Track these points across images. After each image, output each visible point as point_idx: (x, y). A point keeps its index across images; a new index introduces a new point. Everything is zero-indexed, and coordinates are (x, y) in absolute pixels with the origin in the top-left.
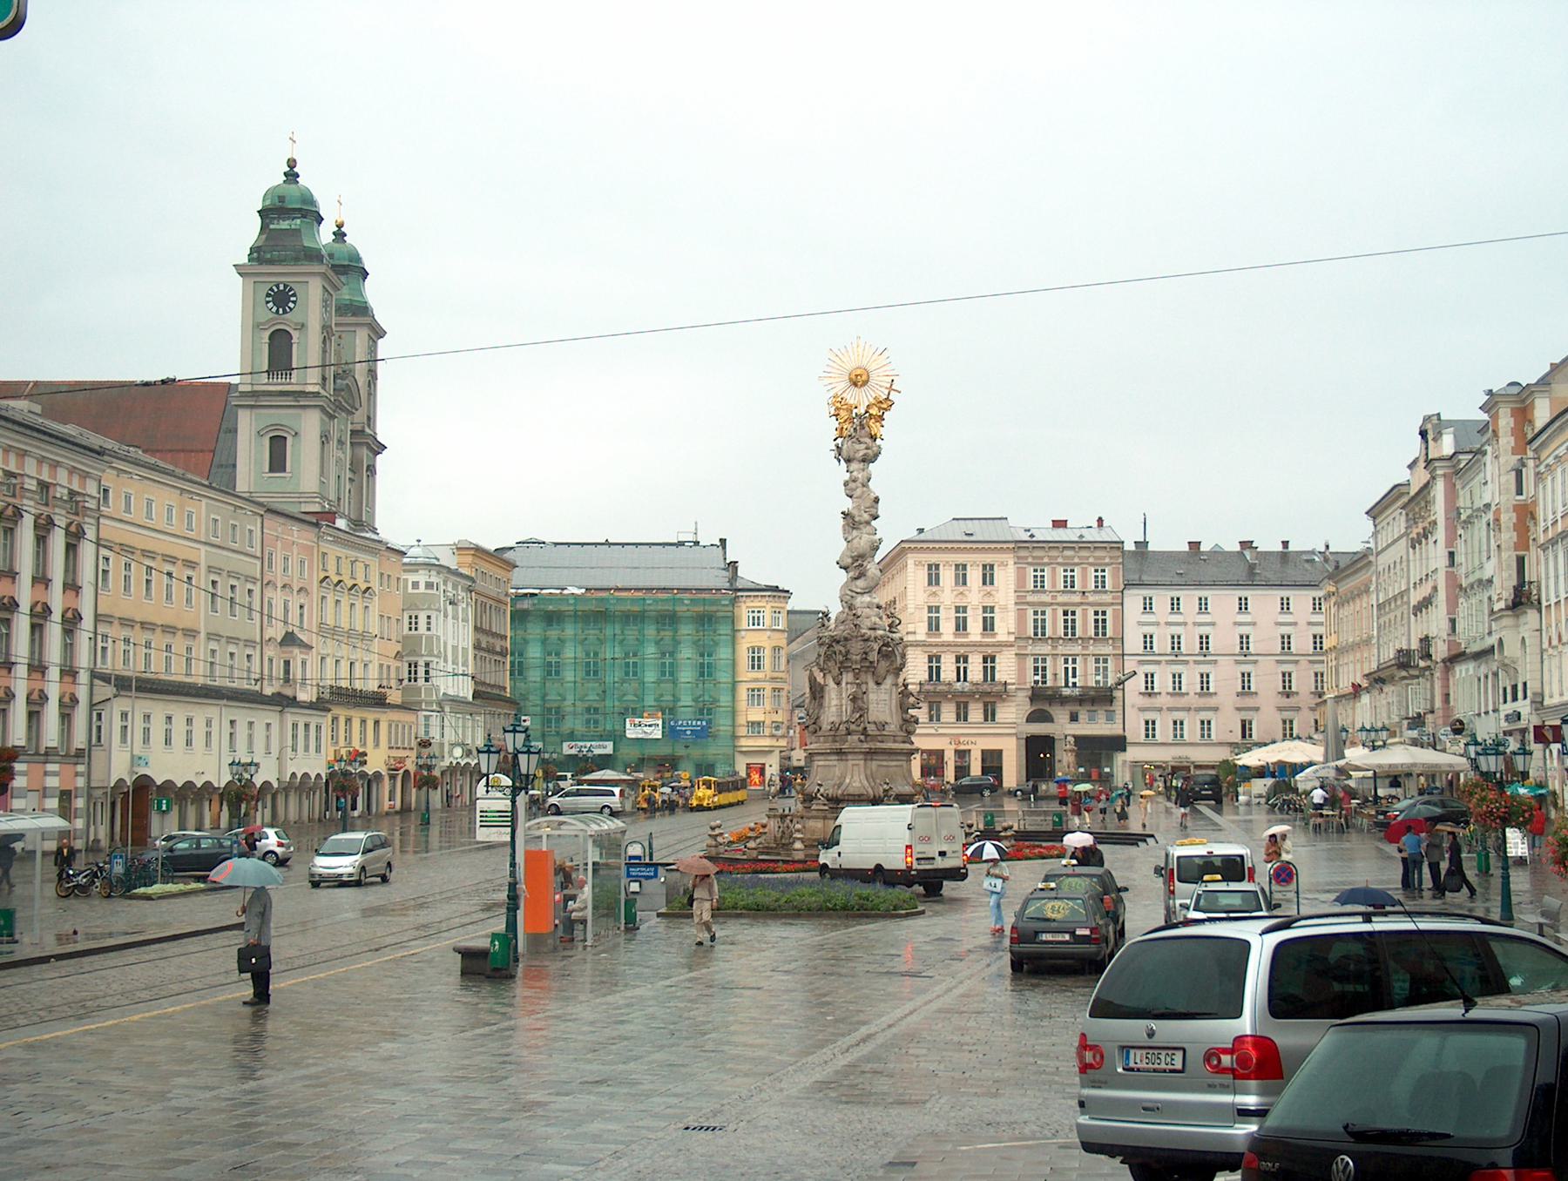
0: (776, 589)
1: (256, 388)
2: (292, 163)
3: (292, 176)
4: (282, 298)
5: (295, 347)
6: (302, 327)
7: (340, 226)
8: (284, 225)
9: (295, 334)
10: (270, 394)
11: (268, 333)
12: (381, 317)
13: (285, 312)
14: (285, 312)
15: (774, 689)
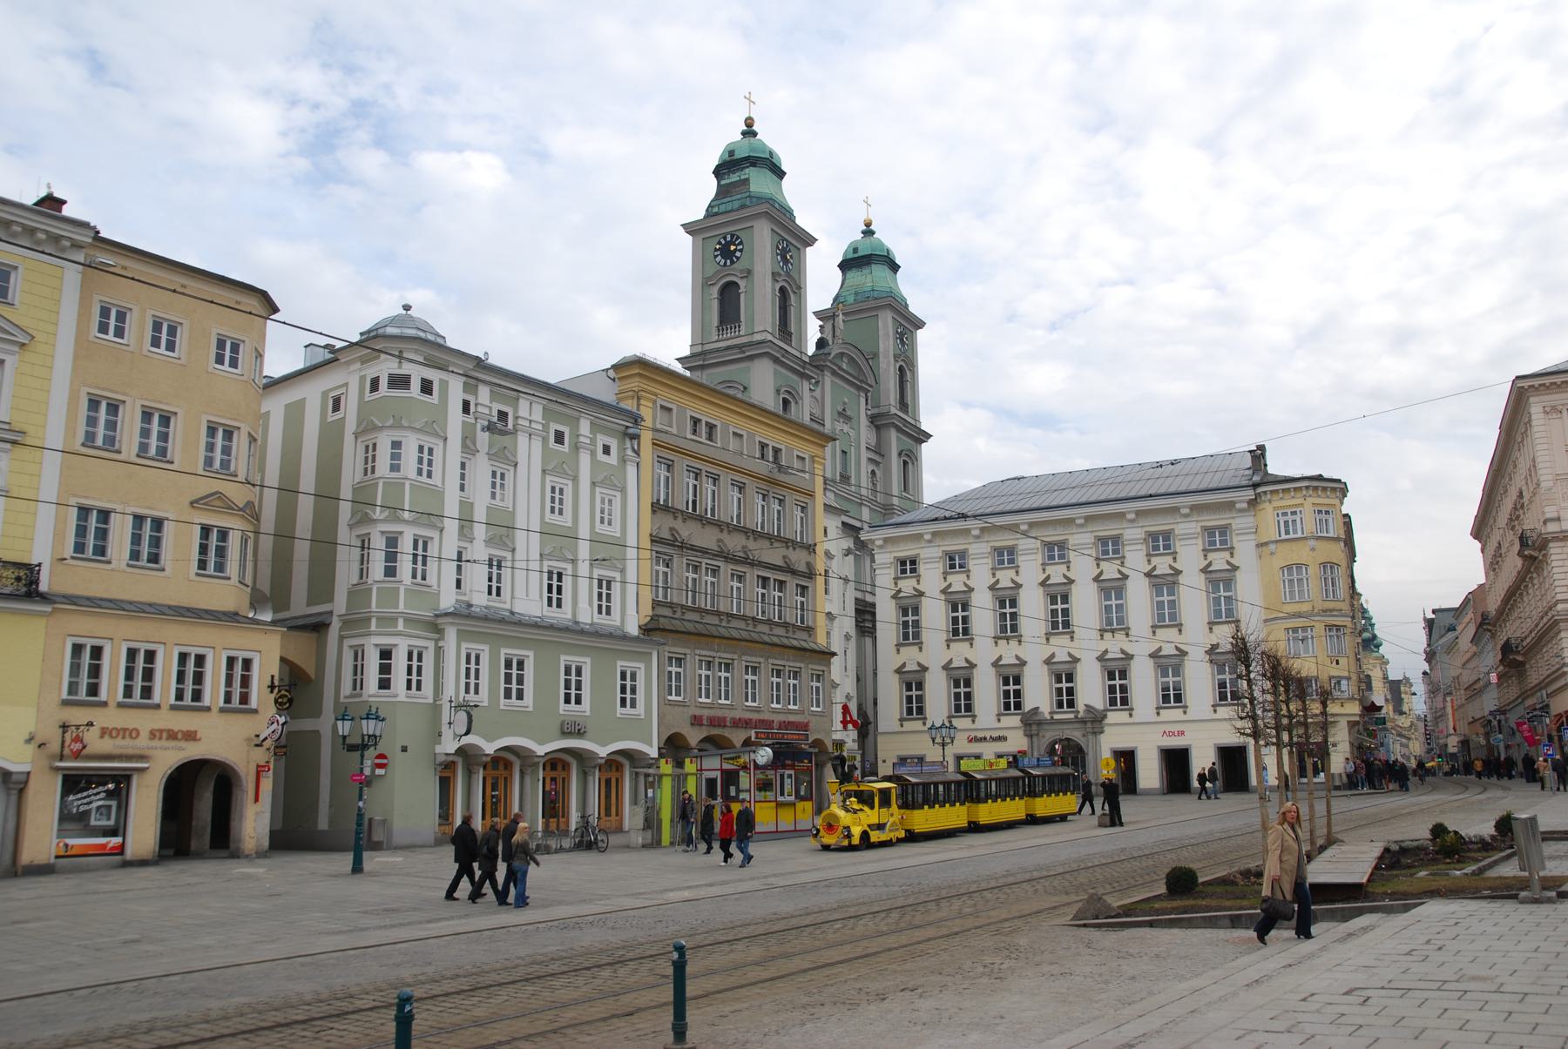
0: (1320, 478)
1: (707, 347)
2: (749, 122)
3: (749, 132)
4: (726, 252)
5: (742, 297)
6: (748, 273)
7: (868, 224)
8: (734, 178)
9: (742, 283)
10: (718, 350)
11: (715, 291)
12: (914, 308)
13: (732, 262)
14: (732, 262)
15: (1329, 627)
